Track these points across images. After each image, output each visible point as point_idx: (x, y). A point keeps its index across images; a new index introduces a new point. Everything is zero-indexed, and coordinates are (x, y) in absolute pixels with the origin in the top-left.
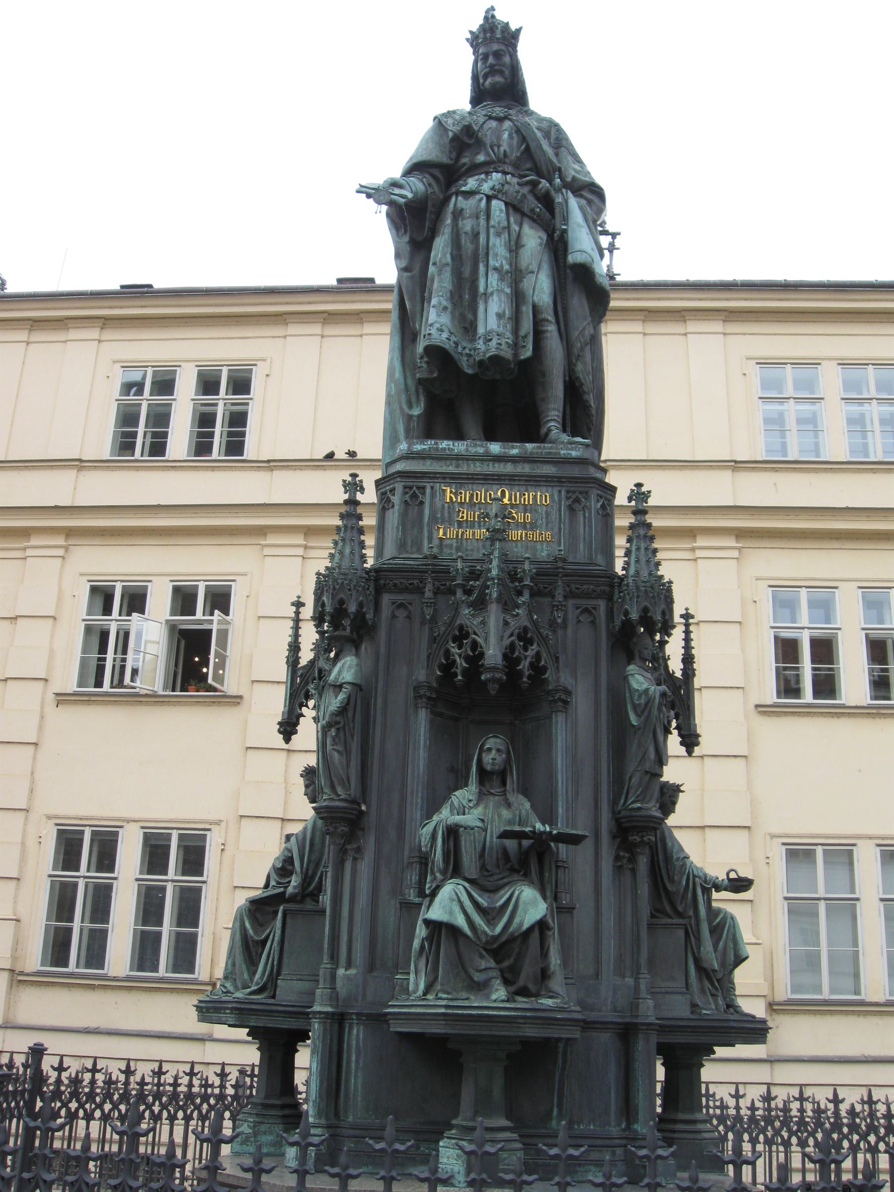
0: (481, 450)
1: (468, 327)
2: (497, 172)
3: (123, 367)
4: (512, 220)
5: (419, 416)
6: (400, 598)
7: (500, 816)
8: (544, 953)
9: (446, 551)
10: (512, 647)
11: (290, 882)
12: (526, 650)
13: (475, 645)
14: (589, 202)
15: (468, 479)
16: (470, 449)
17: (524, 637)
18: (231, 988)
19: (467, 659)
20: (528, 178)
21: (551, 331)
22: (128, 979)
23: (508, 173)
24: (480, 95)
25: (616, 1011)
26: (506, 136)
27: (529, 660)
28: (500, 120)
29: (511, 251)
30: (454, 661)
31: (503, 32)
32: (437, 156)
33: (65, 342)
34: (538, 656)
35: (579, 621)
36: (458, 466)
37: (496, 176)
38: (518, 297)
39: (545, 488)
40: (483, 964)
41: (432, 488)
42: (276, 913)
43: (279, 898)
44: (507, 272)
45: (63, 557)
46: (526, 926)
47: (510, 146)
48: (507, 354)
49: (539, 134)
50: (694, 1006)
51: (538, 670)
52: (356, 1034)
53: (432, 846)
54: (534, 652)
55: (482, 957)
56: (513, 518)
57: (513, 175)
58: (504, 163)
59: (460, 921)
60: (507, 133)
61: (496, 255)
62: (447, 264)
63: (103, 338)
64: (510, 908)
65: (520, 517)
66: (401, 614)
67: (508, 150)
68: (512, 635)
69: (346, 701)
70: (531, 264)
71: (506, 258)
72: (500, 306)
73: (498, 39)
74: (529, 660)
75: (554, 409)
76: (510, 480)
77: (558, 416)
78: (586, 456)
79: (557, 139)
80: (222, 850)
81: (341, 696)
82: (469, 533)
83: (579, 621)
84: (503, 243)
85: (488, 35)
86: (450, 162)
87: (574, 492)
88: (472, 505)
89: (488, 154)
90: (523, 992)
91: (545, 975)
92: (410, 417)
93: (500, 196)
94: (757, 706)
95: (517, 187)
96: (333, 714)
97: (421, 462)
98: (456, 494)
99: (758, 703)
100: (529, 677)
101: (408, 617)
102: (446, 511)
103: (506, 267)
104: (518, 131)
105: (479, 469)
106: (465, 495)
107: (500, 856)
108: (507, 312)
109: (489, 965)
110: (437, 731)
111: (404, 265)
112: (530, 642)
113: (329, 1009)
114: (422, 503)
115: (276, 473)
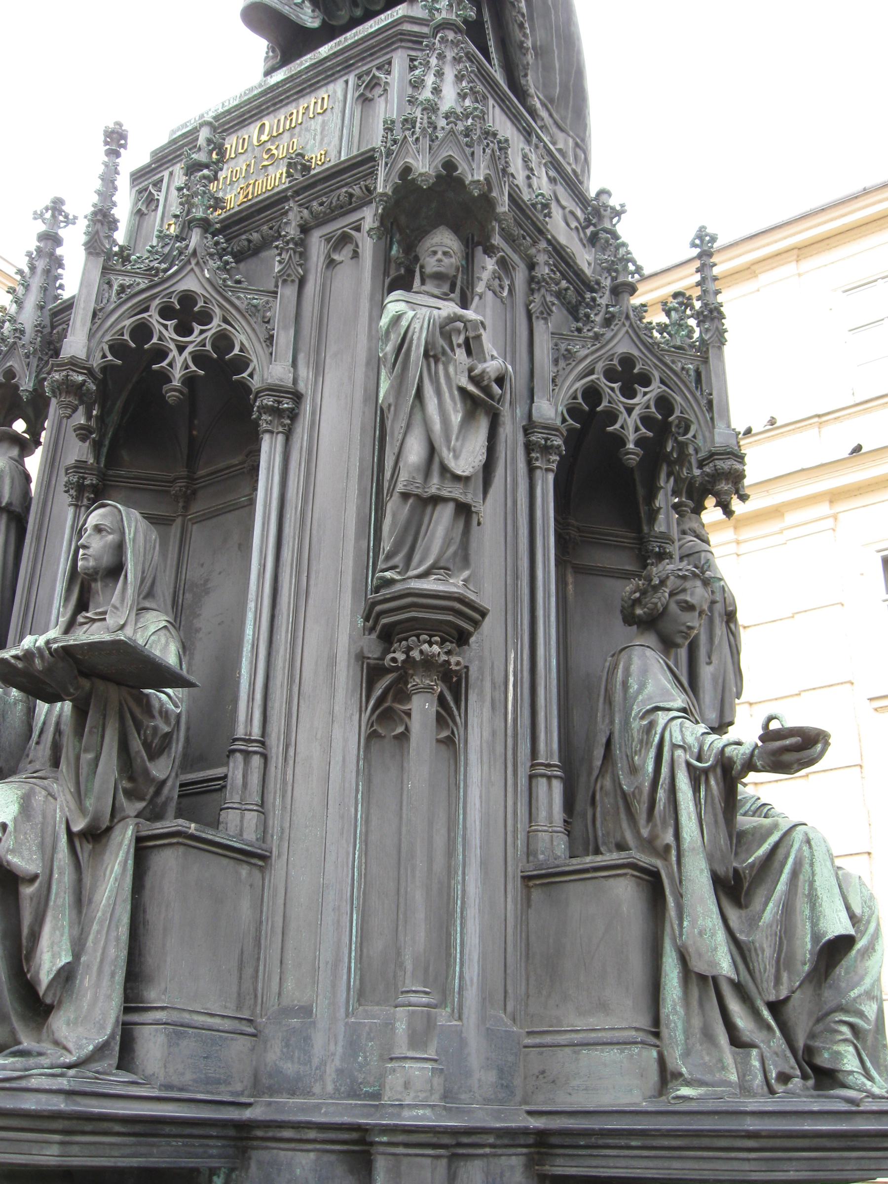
12: (184, 329)
25: (353, 1094)
35: (331, 263)
50: (667, 1076)
100: (189, 380)
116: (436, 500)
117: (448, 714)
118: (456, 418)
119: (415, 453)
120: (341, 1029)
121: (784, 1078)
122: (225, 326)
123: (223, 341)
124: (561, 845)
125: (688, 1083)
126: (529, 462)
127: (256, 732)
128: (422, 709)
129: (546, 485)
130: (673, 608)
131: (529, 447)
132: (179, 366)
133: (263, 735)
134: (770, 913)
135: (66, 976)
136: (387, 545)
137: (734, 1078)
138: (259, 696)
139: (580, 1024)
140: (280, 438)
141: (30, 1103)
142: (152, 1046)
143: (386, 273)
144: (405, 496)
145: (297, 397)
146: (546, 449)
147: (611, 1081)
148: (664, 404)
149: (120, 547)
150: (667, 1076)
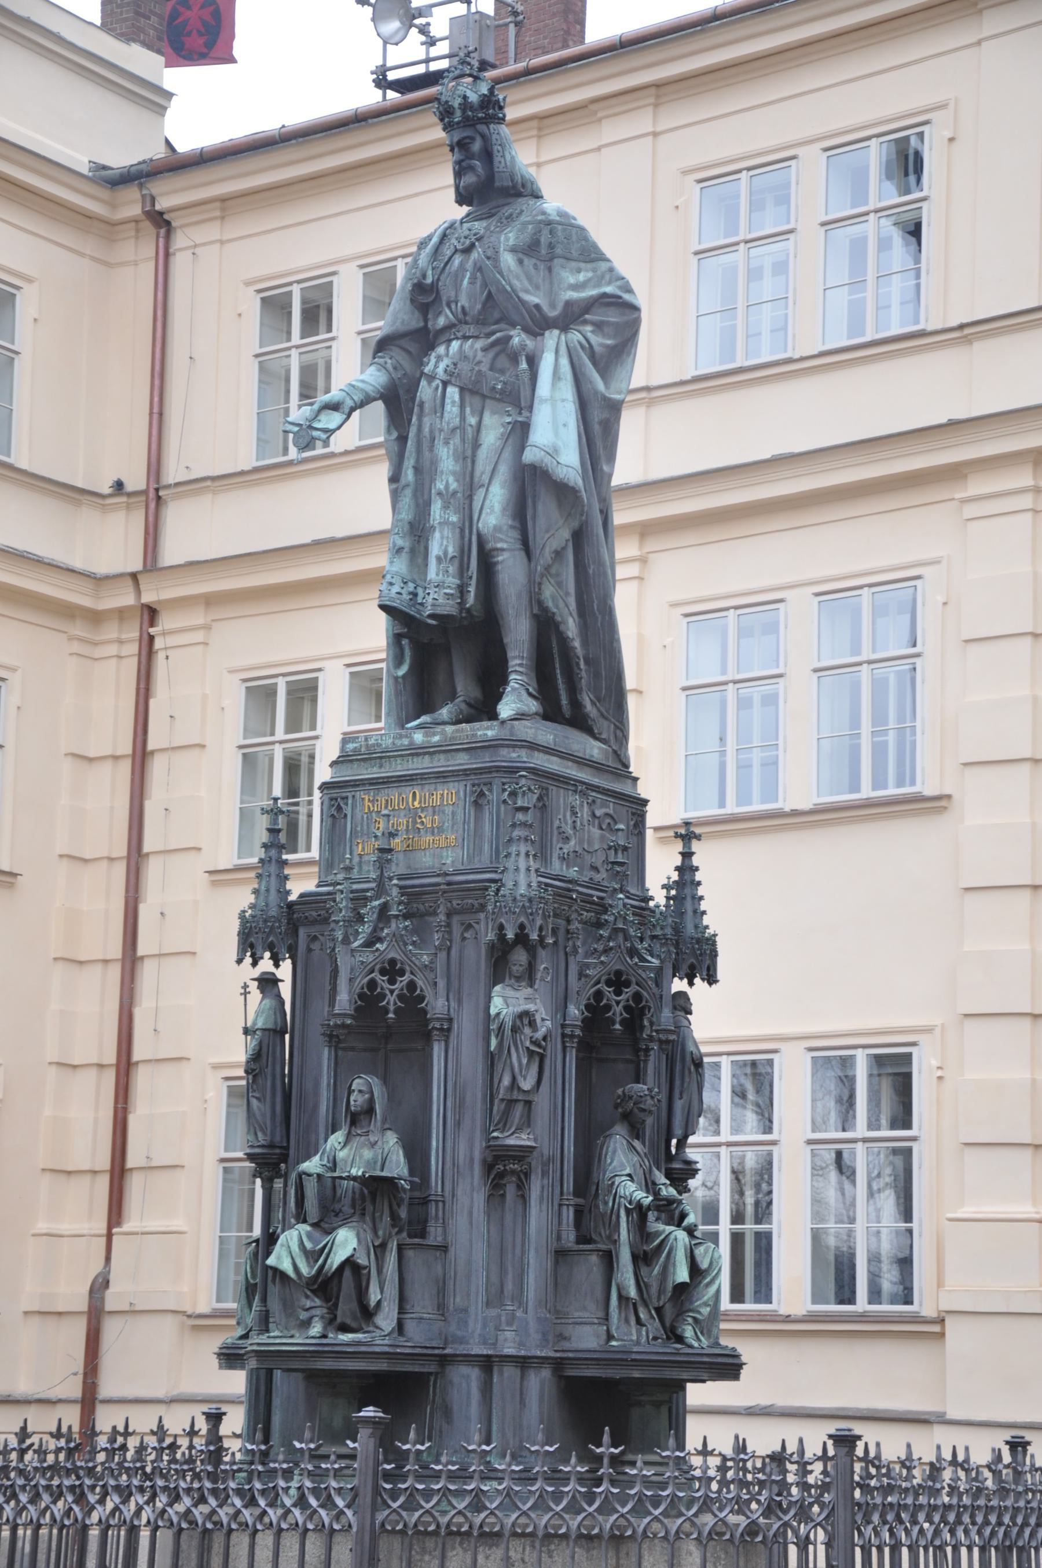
0: (406, 742)
2: (457, 338)
3: (700, 181)
4: (468, 410)
5: (404, 677)
6: (314, 930)
7: (361, 1157)
8: (361, 1292)
9: (365, 868)
10: (372, 984)
12: (392, 982)
14: (599, 326)
15: (383, 783)
16: (397, 741)
17: (392, 970)
20: (494, 338)
21: (502, 562)
22: (812, 1318)
23: (469, 337)
24: (462, 199)
26: (466, 281)
27: (396, 993)
28: (468, 250)
29: (465, 458)
31: (464, 111)
32: (403, 323)
33: (599, 149)
34: (412, 986)
35: (464, 939)
36: (381, 767)
37: (455, 345)
39: (452, 784)
40: (308, 1304)
41: (354, 796)
44: (455, 493)
45: (640, 578)
46: (335, 1267)
47: (471, 296)
49: (508, 260)
51: (412, 999)
54: (405, 983)
55: (307, 1297)
56: (422, 823)
57: (477, 337)
58: (466, 323)
59: (286, 1266)
60: (468, 274)
61: (442, 472)
62: (408, 485)
63: (659, 129)
64: (326, 1251)
65: (427, 821)
67: (467, 305)
68: (372, 971)
69: (257, 1048)
70: (483, 473)
71: (454, 473)
72: (442, 545)
73: (458, 123)
74: (396, 993)
75: (515, 658)
76: (422, 779)
77: (520, 665)
78: (505, 733)
79: (551, 246)
80: (940, 1078)
83: (464, 939)
84: (451, 452)
87: (479, 785)
89: (447, 316)
90: (344, 1329)
91: (367, 1314)
92: (396, 678)
93: (453, 380)
95: (480, 354)
97: (349, 765)
98: (372, 802)
102: (365, 823)
103: (454, 486)
104: (480, 269)
105: (399, 767)
107: (357, 1196)
108: (451, 550)
109: (313, 1304)
112: (402, 972)
114: (346, 815)
115: (977, 346)
116: (517, 1101)
117: (520, 1186)
118: (525, 1061)
119: (506, 1081)
120: (480, 1317)
121: (655, 1338)
122: (412, 977)
123: (412, 986)
124: (572, 1237)
125: (617, 1340)
126: (563, 1042)
127: (440, 1189)
128: (511, 1191)
129: (572, 1056)
130: (636, 1110)
131: (563, 1035)
132: (391, 1001)
133: (443, 1191)
134: (657, 1270)
135: (379, 1303)
136: (496, 1119)
137: (635, 1338)
138: (440, 1174)
139: (576, 1314)
140: (443, 1043)
141: (377, 1349)
142: (410, 1326)
143: (492, 956)
144: (502, 1100)
145: (450, 1020)
146: (572, 1036)
147: (586, 1339)
148: (637, 997)
149: (371, 1100)
150: (610, 1337)
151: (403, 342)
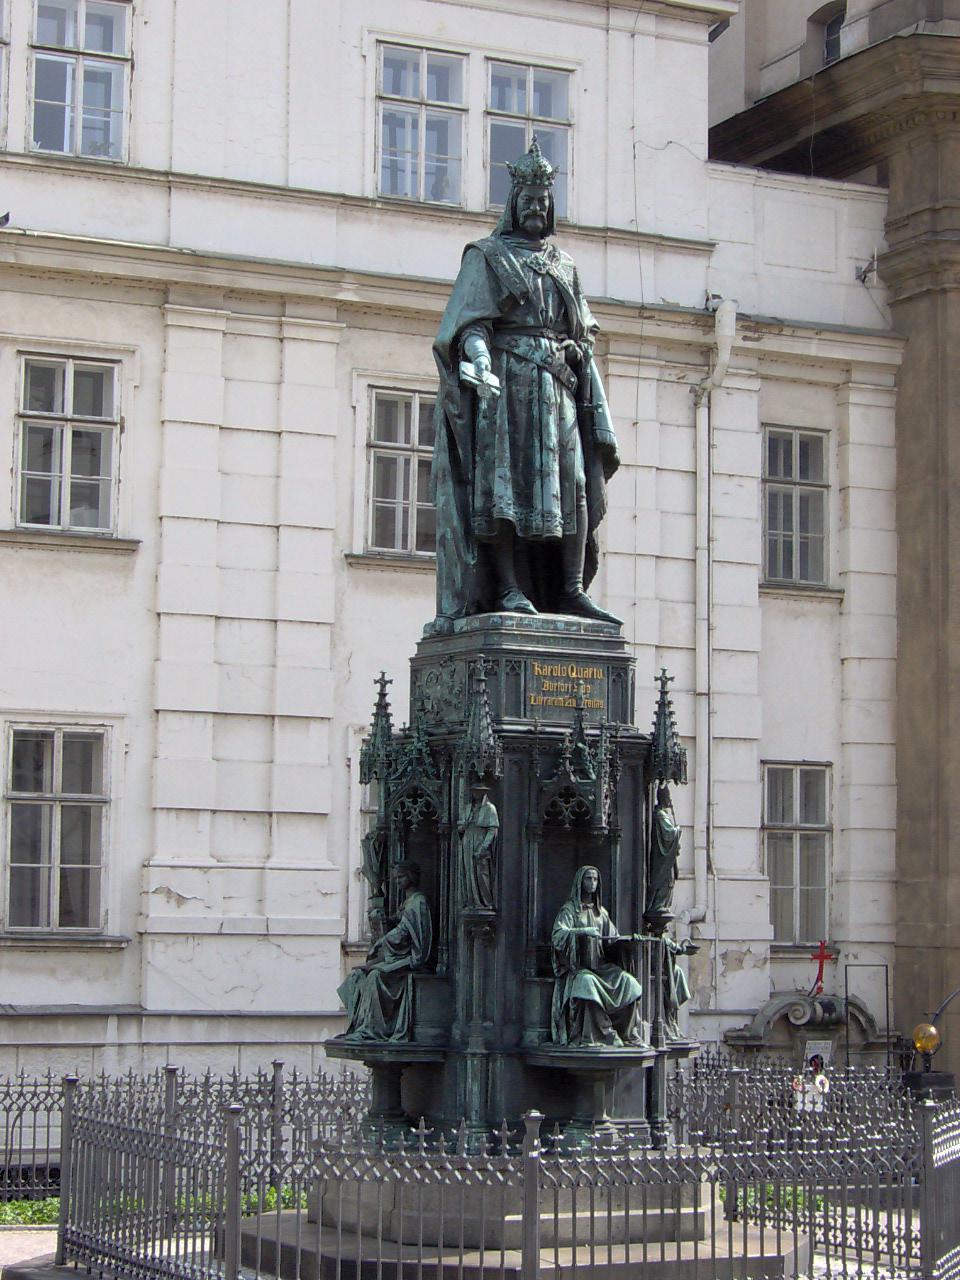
1: (525, 496)
2: (543, 337)
11: (410, 953)
13: (580, 805)
18: (372, 1035)
19: (573, 813)
30: (561, 813)
38: (566, 474)
42: (404, 978)
43: (407, 969)
48: (559, 532)
52: (500, 1064)
53: (566, 948)
55: (606, 1019)
59: (597, 998)
66: (515, 768)
81: (489, 837)
82: (551, 699)
85: (538, 181)
86: (499, 315)
88: (552, 677)
92: (466, 566)
94: (347, 556)
96: (484, 849)
99: (347, 552)
101: (520, 770)
106: (547, 670)
110: (543, 856)
111: (456, 412)
113: (484, 1051)
114: (518, 674)
151: (485, 323)
